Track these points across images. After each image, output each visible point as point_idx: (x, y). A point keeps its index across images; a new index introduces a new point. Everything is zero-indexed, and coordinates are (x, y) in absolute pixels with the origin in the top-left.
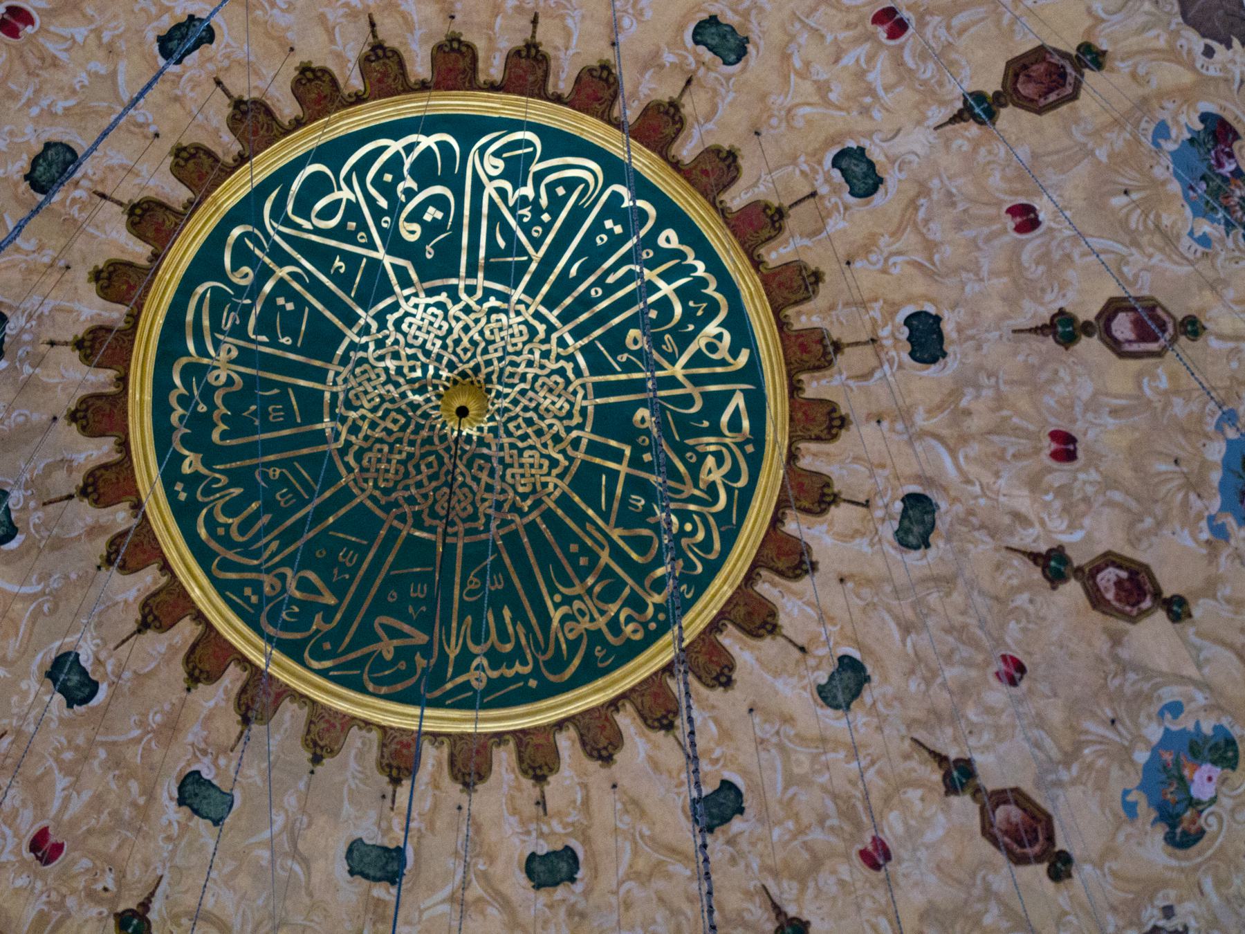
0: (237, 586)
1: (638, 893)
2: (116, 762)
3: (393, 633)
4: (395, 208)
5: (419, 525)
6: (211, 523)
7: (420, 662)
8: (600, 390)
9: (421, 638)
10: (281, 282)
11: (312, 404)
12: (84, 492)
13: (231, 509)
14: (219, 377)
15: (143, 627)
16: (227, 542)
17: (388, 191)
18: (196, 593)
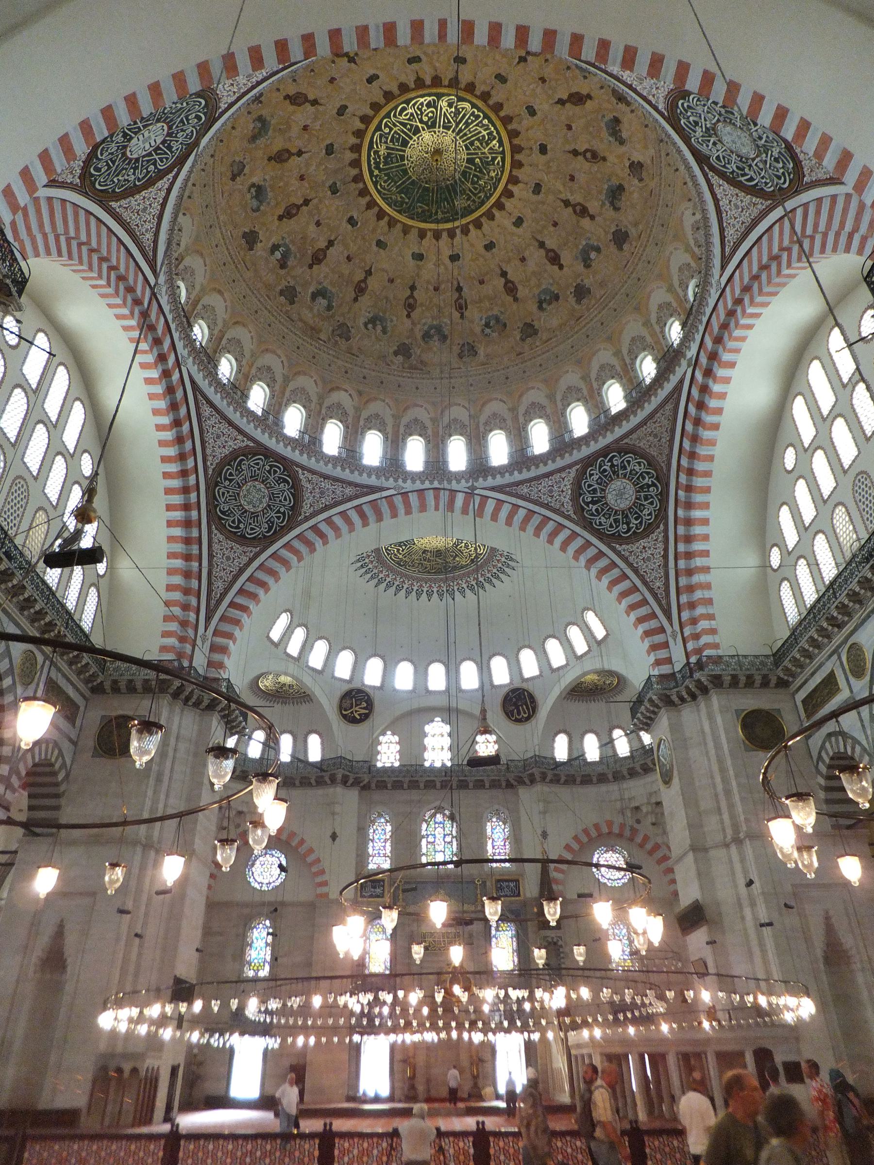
0: (387, 199)
1: (472, 263)
2: (363, 238)
3: (421, 207)
4: (422, 113)
5: (426, 183)
6: (381, 185)
7: (427, 213)
8: (468, 154)
9: (427, 208)
10: (395, 132)
11: (402, 158)
12: (353, 181)
13: (385, 182)
14: (381, 153)
15: (367, 209)
16: (384, 189)
17: (420, 110)
18: (378, 201)
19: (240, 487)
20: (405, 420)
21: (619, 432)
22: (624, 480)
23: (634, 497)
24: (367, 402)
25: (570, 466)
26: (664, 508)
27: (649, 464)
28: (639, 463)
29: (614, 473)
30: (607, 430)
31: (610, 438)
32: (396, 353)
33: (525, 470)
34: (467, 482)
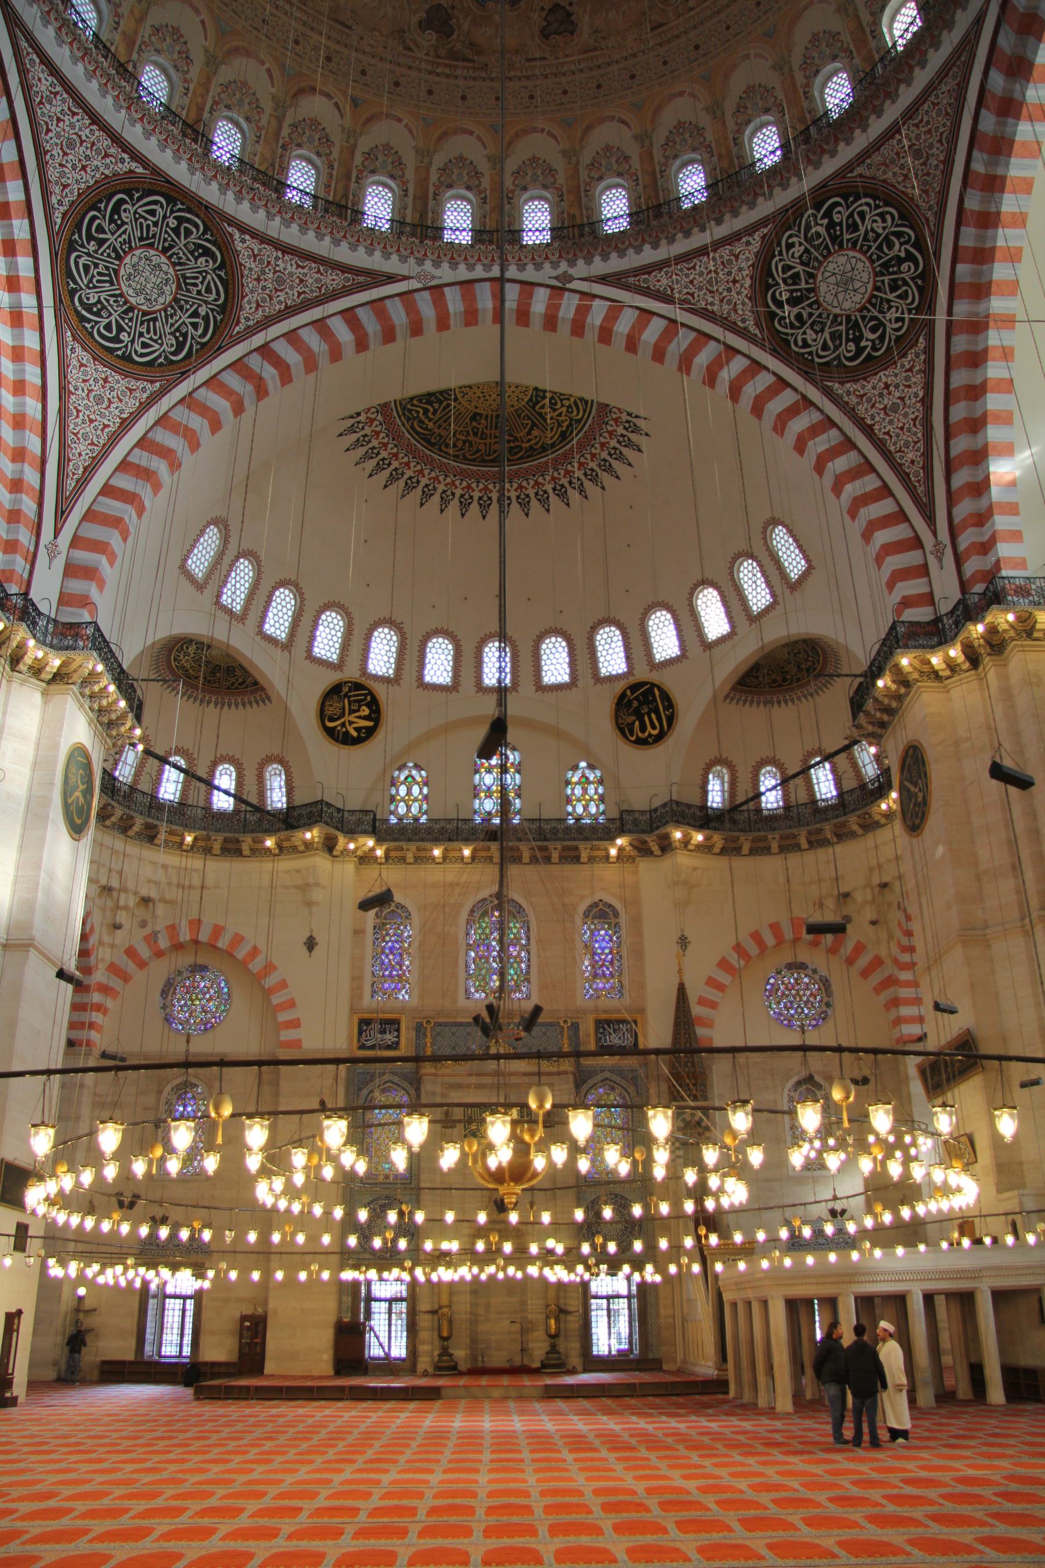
19: (119, 258)
20: (439, 160)
21: (846, 153)
22: (851, 254)
23: (870, 287)
24: (368, 120)
25: (750, 230)
26: (928, 303)
27: (902, 217)
28: (882, 215)
29: (834, 239)
30: (823, 151)
31: (830, 166)
32: (423, 25)
33: (664, 242)
34: (555, 265)
